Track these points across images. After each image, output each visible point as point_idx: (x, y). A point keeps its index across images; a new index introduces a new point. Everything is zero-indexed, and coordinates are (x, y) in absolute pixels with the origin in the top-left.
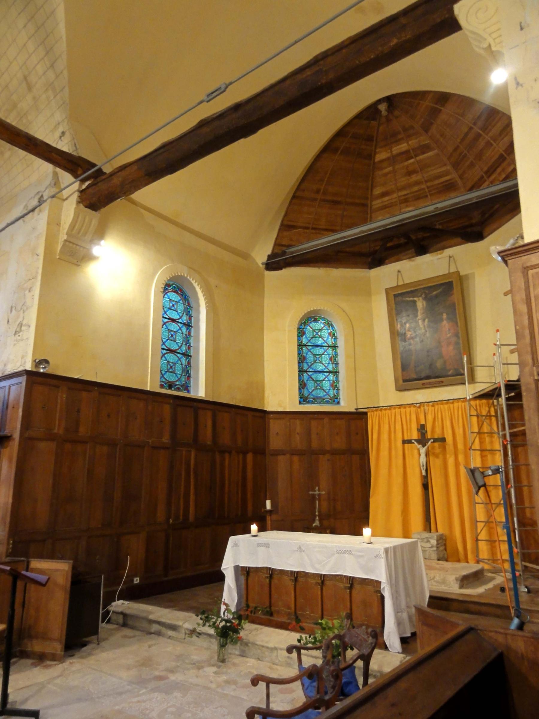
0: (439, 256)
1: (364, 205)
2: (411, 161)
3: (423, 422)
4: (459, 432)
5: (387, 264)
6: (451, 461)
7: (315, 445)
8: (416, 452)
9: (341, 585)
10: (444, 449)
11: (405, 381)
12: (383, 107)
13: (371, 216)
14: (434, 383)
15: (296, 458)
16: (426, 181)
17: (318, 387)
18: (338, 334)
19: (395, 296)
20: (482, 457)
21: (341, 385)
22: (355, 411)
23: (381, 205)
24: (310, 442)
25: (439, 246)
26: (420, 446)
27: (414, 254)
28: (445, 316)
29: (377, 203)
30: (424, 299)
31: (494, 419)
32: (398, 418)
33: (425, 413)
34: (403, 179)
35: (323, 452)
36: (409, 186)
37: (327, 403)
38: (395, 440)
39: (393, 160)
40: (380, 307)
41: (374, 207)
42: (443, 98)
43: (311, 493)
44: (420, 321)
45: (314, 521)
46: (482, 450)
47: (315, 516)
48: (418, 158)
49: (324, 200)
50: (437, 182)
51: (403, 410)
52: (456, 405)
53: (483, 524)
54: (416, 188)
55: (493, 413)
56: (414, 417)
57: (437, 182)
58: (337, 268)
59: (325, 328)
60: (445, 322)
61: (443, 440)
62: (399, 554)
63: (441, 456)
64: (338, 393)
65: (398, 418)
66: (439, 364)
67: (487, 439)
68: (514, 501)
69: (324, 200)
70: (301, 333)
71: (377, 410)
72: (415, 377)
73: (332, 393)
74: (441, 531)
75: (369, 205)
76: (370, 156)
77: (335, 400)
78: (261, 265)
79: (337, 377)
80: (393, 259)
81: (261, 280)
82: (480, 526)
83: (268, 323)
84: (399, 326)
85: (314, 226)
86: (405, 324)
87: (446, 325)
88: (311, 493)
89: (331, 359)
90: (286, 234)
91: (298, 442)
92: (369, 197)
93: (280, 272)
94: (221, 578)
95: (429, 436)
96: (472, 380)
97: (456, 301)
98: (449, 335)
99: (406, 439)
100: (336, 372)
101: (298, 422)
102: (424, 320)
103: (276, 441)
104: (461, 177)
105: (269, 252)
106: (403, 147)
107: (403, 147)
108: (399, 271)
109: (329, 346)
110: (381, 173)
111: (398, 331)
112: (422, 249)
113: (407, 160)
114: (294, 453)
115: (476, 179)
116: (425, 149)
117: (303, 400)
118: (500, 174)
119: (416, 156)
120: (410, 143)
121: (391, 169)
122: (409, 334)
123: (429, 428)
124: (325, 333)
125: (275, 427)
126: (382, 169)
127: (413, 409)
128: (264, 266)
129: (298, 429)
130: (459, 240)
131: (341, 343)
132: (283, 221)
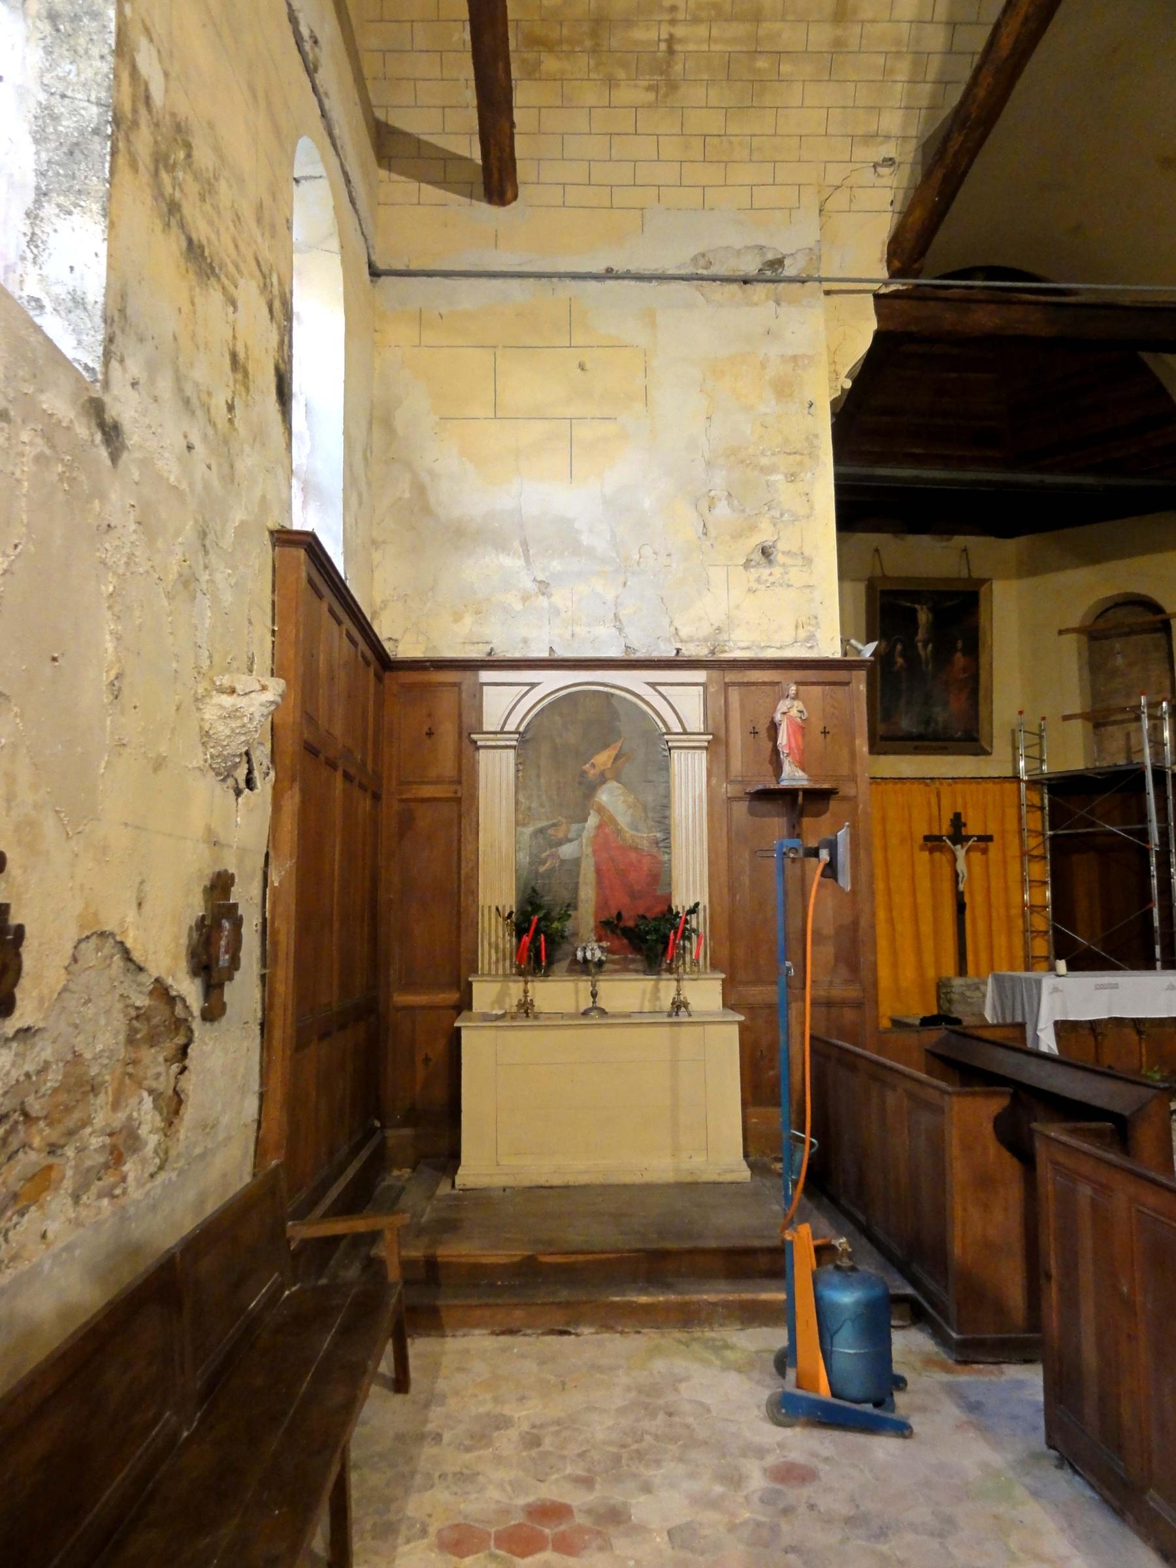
0: (945, 544)
2: (953, 375)
11: (884, 738)
19: (884, 593)
28: (960, 644)
30: (930, 609)
52: (984, 786)
60: (959, 655)
68: (1156, 924)
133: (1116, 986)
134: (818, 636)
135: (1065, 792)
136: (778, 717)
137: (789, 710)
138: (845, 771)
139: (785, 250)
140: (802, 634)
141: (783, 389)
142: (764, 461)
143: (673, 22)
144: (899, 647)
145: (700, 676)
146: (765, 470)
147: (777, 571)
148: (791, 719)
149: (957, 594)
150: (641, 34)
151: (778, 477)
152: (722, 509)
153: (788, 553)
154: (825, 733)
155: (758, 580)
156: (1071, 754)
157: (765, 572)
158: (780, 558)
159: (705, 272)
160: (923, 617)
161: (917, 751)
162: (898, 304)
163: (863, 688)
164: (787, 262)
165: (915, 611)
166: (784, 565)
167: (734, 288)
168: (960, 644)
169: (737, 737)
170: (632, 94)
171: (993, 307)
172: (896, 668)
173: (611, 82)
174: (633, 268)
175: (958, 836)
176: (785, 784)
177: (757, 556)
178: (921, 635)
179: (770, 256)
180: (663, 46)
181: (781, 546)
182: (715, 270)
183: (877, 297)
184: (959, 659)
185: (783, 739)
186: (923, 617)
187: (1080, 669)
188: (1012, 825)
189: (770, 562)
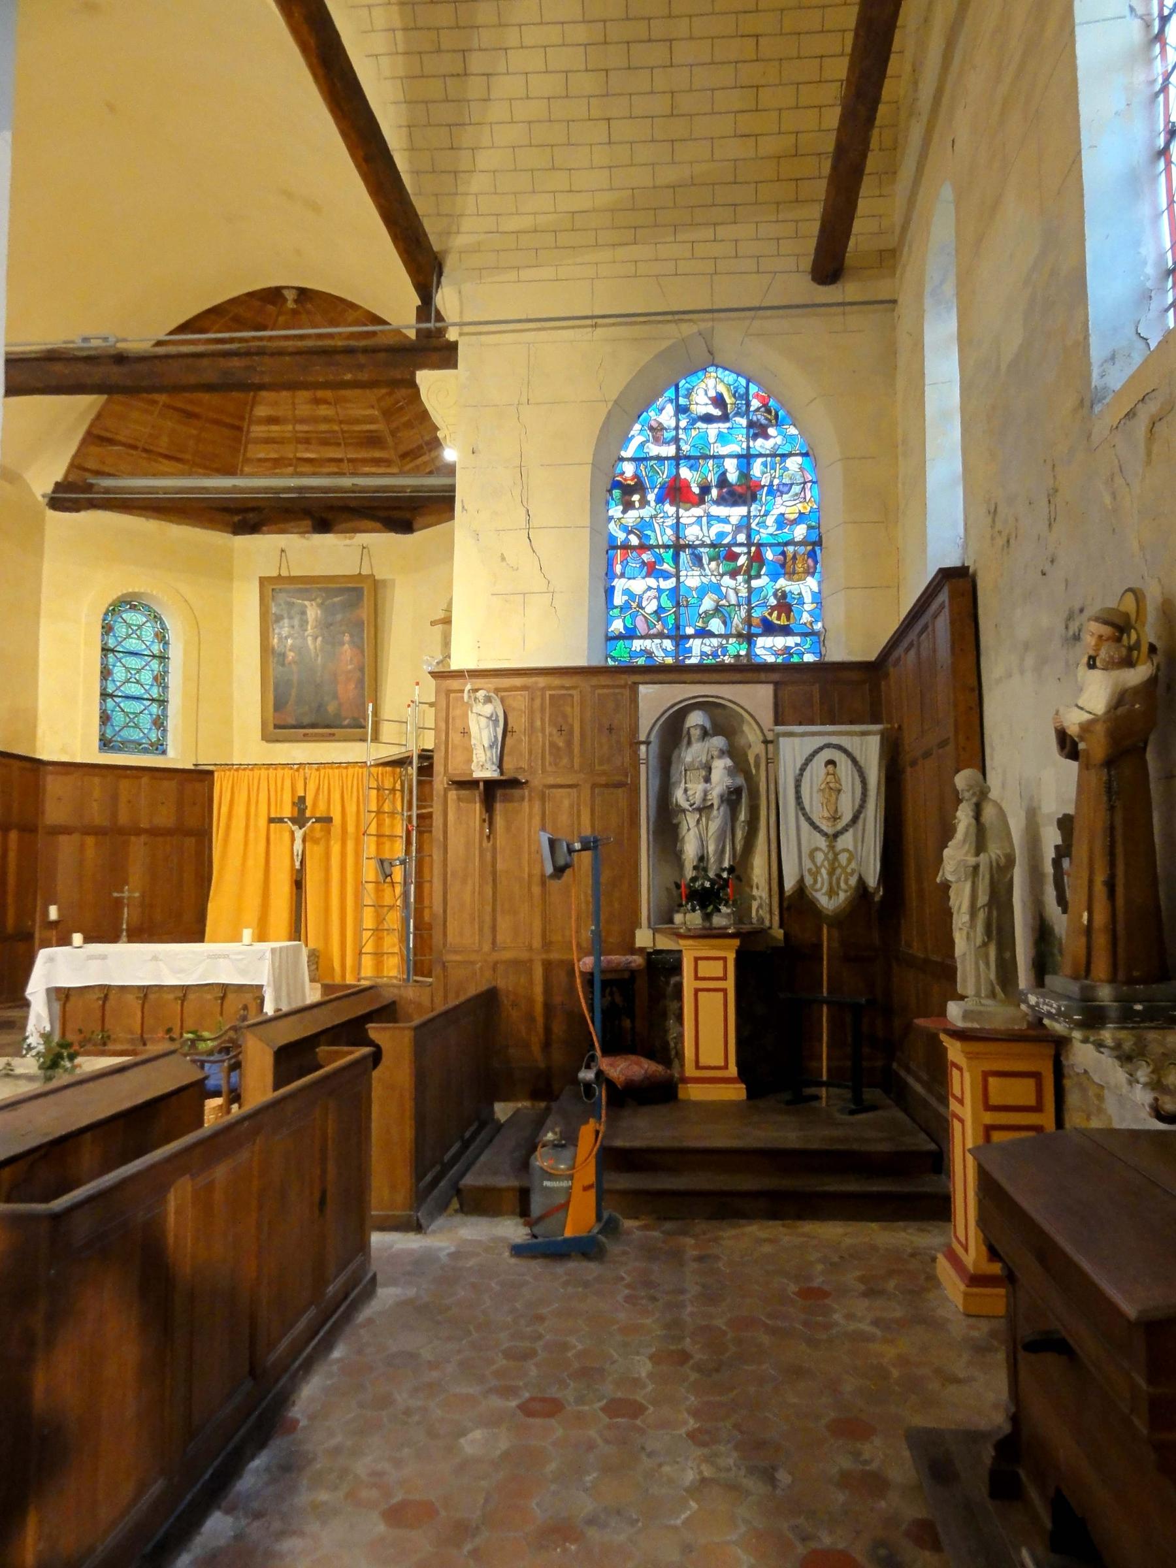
0: (348, 542)
1: (239, 429)
4: (351, 809)
5: (263, 533)
6: (336, 848)
7: (123, 819)
8: (287, 835)
9: (209, 997)
10: (329, 832)
11: (276, 727)
12: (290, 296)
13: (246, 447)
14: (322, 735)
15: (90, 841)
16: (341, 422)
17: (131, 724)
18: (171, 636)
20: (379, 845)
21: (170, 724)
22: (193, 768)
23: (264, 435)
24: (114, 815)
25: (349, 525)
26: (295, 828)
27: (310, 529)
28: (347, 638)
29: (258, 431)
30: (320, 606)
31: (398, 794)
32: (264, 785)
33: (305, 779)
34: (308, 407)
35: (138, 832)
36: (315, 420)
38: (256, 815)
40: (246, 603)
41: (252, 435)
43: (115, 895)
44: (310, 639)
46: (379, 836)
47: (122, 931)
49: (168, 407)
50: (357, 428)
51: (272, 772)
52: (351, 771)
53: (370, 933)
54: (323, 427)
55: (398, 787)
56: (288, 783)
57: (357, 428)
58: (179, 523)
59: (148, 624)
60: (347, 646)
61: (329, 820)
62: (284, 955)
63: (323, 842)
65: (264, 785)
66: (331, 708)
67: (387, 821)
69: (168, 407)
70: (107, 629)
71: (229, 770)
72: (293, 722)
73: (153, 736)
74: (312, 945)
75: (245, 429)
77: (159, 748)
78: (40, 498)
79: (165, 709)
80: (274, 527)
81: (39, 526)
82: (366, 935)
83: (48, 604)
84: (276, 640)
85: (147, 447)
86: (286, 638)
87: (347, 650)
88: (115, 895)
89: (155, 678)
90: (94, 450)
91: (96, 814)
92: (247, 416)
93: (74, 515)
94: (26, 1004)
95: (308, 814)
96: (376, 738)
97: (365, 618)
98: (350, 667)
99: (273, 815)
100: (164, 701)
101: (97, 780)
102: (315, 638)
103: (55, 812)
104: (393, 433)
105: (59, 477)
108: (283, 551)
109: (154, 656)
111: (273, 648)
112: (323, 525)
114: (88, 831)
115: (411, 447)
117: (106, 744)
122: (291, 655)
123: (309, 802)
124: (148, 633)
125: (54, 786)
127: (288, 773)
128: (46, 500)
129: (97, 793)
130: (378, 525)
131: (176, 653)
132: (92, 425)
133: (104, 957)
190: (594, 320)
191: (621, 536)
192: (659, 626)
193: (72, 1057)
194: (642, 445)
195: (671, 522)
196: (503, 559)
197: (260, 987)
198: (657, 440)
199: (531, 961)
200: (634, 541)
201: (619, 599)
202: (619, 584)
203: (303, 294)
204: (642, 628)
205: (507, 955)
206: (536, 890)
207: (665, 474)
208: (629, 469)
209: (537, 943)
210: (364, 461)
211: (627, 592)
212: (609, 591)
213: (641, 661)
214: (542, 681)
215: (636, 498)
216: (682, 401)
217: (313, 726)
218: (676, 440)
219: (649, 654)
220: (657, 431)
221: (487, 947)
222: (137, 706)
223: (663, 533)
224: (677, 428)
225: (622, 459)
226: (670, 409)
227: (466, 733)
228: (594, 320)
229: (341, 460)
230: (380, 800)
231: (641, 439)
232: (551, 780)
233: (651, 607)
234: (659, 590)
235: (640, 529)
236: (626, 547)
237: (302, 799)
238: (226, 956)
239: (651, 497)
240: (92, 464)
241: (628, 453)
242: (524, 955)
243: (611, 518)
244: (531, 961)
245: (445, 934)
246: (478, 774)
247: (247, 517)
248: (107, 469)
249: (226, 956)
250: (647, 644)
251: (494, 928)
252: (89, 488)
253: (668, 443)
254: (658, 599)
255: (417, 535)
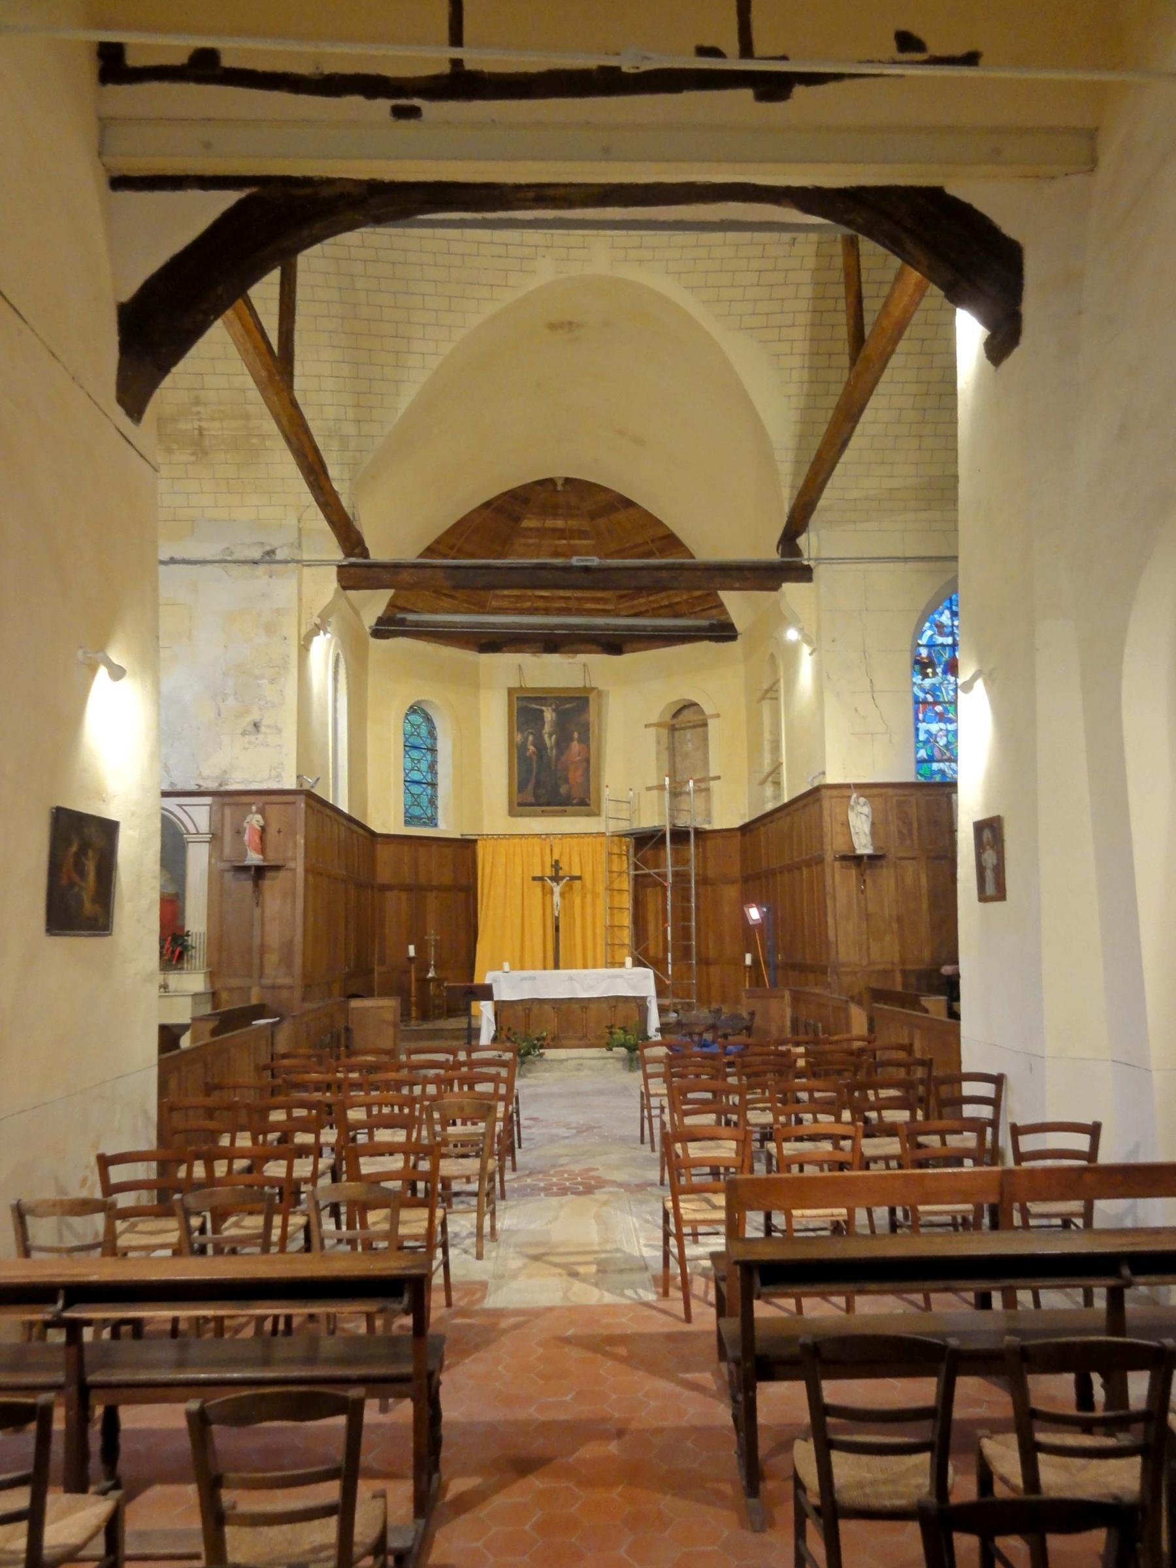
0: (571, 660)
2: (564, 542)
3: (556, 857)
6: (578, 901)
7: (423, 880)
9: (604, 1006)
11: (520, 805)
12: (560, 483)
15: (404, 895)
18: (439, 733)
21: (440, 803)
28: (576, 735)
31: (624, 858)
35: (429, 888)
37: (425, 824)
39: (541, 532)
42: (628, 503)
45: (428, 971)
48: (572, 542)
58: (446, 645)
64: (436, 813)
66: (563, 790)
76: (518, 519)
77: (432, 821)
101: (406, 848)
102: (550, 736)
103: (384, 875)
106: (560, 524)
107: (560, 524)
110: (523, 541)
113: (559, 538)
116: (583, 534)
118: (663, 599)
119: (571, 538)
120: (570, 522)
121: (537, 541)
124: (424, 731)
125: (384, 853)
126: (525, 537)
127: (536, 840)
129: (406, 859)
130: (594, 647)
131: (444, 746)
133: (533, 978)
134: (283, 774)
135: (646, 842)
136: (245, 824)
137: (255, 820)
138: (290, 854)
139: (275, 544)
140: (274, 773)
141: (270, 629)
142: (257, 672)
143: (200, 420)
144: (531, 738)
145: (208, 800)
146: (256, 678)
147: (260, 736)
148: (252, 827)
149: (572, 699)
150: (184, 426)
151: (265, 681)
152: (231, 701)
153: (268, 726)
154: (279, 832)
155: (250, 743)
156: (652, 817)
157: (253, 738)
158: (263, 729)
159: (229, 558)
160: (549, 715)
161: (544, 814)
162: (353, 570)
163: (303, 805)
164: (277, 551)
165: (542, 711)
166: (265, 734)
167: (246, 568)
168: (576, 735)
169: (228, 836)
170: (183, 456)
171: (413, 570)
172: (528, 754)
173: (169, 451)
174: (187, 556)
175: (556, 879)
176: (247, 863)
177: (251, 728)
178: (547, 728)
179: (268, 548)
180: (196, 432)
181: (264, 722)
182: (237, 556)
183: (340, 567)
184: (575, 746)
185: (246, 838)
186: (549, 715)
187: (658, 753)
188: (602, 868)
189: (258, 731)
190: (906, 559)
191: (921, 695)
192: (948, 754)
193: (542, 1047)
194: (931, 637)
195: (952, 687)
196: (856, 710)
197: (644, 999)
198: (942, 634)
199: (893, 970)
200: (930, 698)
201: (922, 737)
202: (923, 726)
203: (568, 481)
204: (937, 755)
205: (877, 968)
206: (895, 926)
207: (946, 656)
208: (924, 652)
209: (896, 959)
210: (588, 600)
211: (928, 732)
212: (917, 729)
213: (938, 778)
214: (890, 791)
215: (929, 670)
216: (954, 608)
217: (548, 804)
218: (952, 634)
219: (942, 772)
220: (940, 627)
221: (864, 963)
222: (416, 789)
223: (948, 693)
224: (953, 626)
225: (920, 645)
226: (947, 613)
227: (846, 824)
228: (906, 559)
229: (568, 598)
230: (610, 861)
231: (929, 633)
232: (901, 855)
233: (942, 742)
234: (948, 731)
235: (934, 690)
236: (925, 702)
237: (557, 862)
238: (621, 977)
239: (939, 670)
240: (400, 603)
241: (924, 640)
242: (889, 967)
243: (914, 684)
244: (893, 970)
245: (837, 952)
246: (859, 851)
247: (491, 642)
248: (409, 607)
249: (621, 977)
250: (942, 765)
251: (868, 948)
252: (402, 622)
253: (947, 635)
254: (946, 736)
255: (626, 658)
